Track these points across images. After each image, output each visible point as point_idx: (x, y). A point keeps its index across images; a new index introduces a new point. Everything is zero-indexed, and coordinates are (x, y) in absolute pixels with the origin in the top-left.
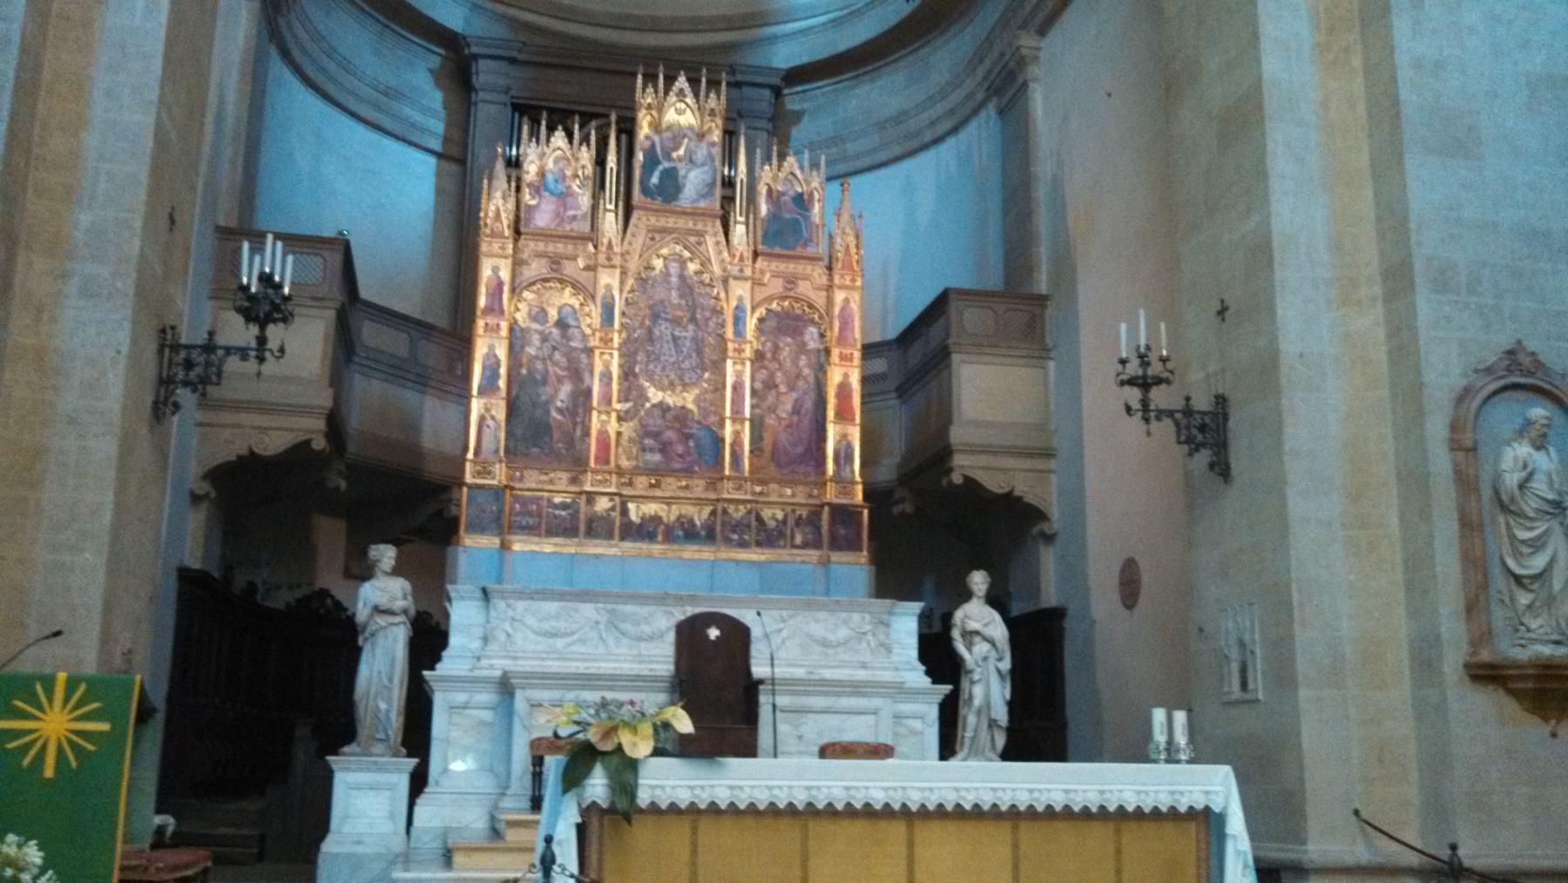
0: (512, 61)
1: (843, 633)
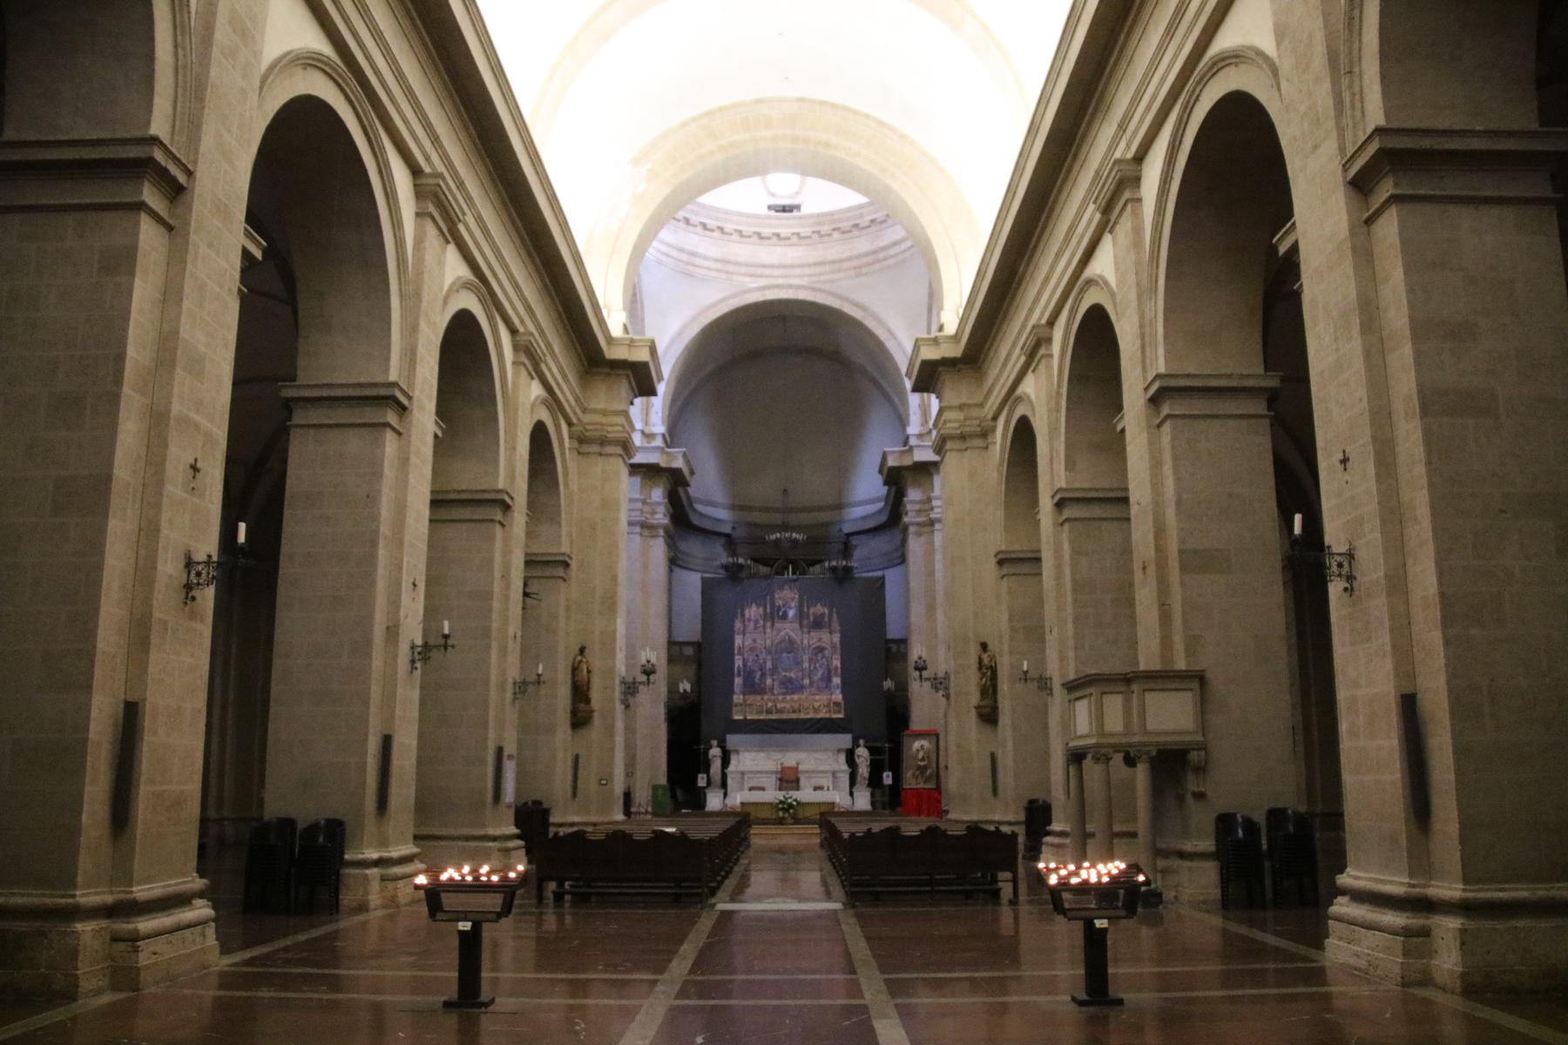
0: (749, 543)
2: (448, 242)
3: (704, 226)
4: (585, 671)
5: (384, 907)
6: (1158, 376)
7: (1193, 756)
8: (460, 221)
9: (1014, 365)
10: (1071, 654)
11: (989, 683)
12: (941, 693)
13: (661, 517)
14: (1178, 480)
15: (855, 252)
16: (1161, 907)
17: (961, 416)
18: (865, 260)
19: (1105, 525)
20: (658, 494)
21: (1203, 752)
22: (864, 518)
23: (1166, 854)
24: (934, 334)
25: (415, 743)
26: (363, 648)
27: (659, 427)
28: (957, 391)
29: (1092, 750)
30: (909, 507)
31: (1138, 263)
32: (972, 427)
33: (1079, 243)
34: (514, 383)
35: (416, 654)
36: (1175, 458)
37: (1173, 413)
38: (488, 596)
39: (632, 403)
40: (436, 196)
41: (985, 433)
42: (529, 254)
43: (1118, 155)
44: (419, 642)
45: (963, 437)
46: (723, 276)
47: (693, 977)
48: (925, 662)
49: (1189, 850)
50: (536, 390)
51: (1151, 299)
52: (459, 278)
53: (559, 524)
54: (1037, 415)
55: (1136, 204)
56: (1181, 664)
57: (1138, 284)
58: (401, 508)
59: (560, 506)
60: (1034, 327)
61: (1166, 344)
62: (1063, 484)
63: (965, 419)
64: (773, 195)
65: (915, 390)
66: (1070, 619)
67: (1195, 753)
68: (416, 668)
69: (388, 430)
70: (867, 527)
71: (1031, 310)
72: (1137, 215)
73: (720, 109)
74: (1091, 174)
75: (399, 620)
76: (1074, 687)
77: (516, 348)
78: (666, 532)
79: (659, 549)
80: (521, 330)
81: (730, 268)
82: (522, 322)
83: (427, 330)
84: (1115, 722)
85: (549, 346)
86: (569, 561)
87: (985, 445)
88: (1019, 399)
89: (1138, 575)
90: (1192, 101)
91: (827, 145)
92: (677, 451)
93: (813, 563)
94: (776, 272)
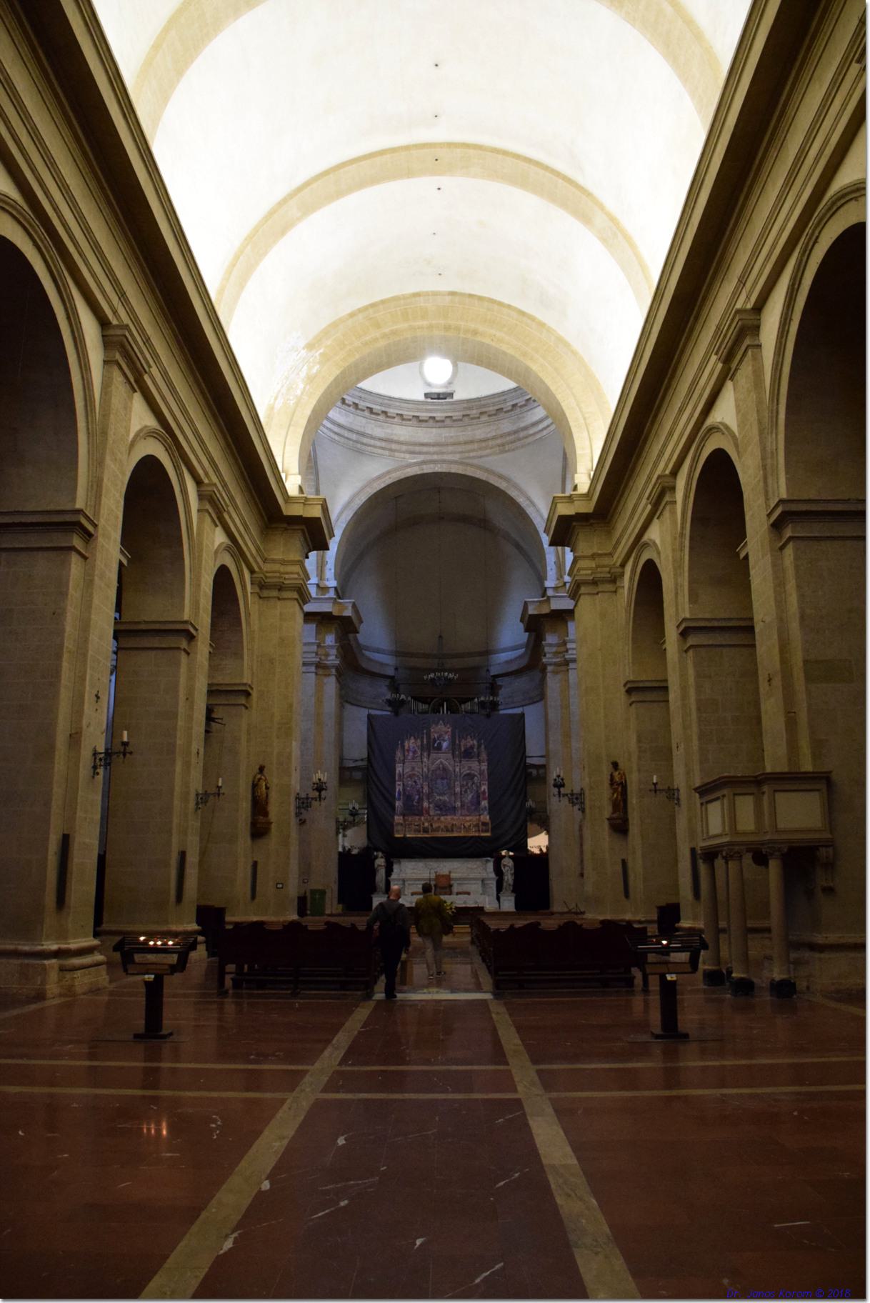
1: (475, 866)
2: (135, 391)
3: (371, 410)
4: (264, 787)
5: (61, 995)
6: (781, 501)
7: (823, 850)
8: (146, 372)
9: (641, 514)
10: (697, 767)
11: (619, 797)
12: (577, 807)
13: (333, 659)
14: (802, 597)
15: (499, 432)
16: (795, 996)
17: (593, 564)
18: (508, 438)
19: (725, 650)
20: (330, 639)
21: (830, 850)
22: (507, 662)
23: (798, 946)
24: (569, 492)
25: (97, 842)
26: (48, 752)
27: (332, 583)
28: (588, 543)
29: (725, 848)
30: (546, 649)
31: (759, 402)
32: (603, 573)
33: (701, 396)
34: (199, 528)
35: (97, 761)
36: (798, 576)
37: (796, 535)
38: (174, 715)
39: (307, 557)
40: (122, 346)
41: (614, 579)
42: (214, 416)
43: (739, 306)
44: (101, 749)
45: (594, 583)
46: (387, 453)
47: (344, 1068)
48: (562, 779)
49: (820, 942)
50: (219, 537)
51: (772, 433)
52: (146, 427)
53: (242, 658)
54: (663, 556)
55: (755, 350)
56: (807, 766)
57: (760, 422)
58: (85, 626)
59: (242, 642)
60: (659, 477)
61: (787, 473)
62: (688, 616)
63: (597, 567)
64: (429, 385)
65: (551, 544)
66: (695, 738)
67: (824, 849)
68: (98, 774)
69: (73, 553)
70: (510, 670)
71: (656, 465)
72: (758, 359)
73: (383, 302)
74: (713, 328)
75: (81, 728)
76: (707, 791)
77: (201, 497)
78: (337, 669)
79: (331, 685)
80: (206, 481)
81: (394, 446)
82: (207, 474)
83: (113, 466)
84: (747, 822)
85: (232, 498)
86: (251, 691)
87: (614, 589)
88: (646, 545)
89: (763, 687)
90: (811, 244)
91: (475, 333)
92: (347, 602)
93: (464, 701)
94: (431, 449)
